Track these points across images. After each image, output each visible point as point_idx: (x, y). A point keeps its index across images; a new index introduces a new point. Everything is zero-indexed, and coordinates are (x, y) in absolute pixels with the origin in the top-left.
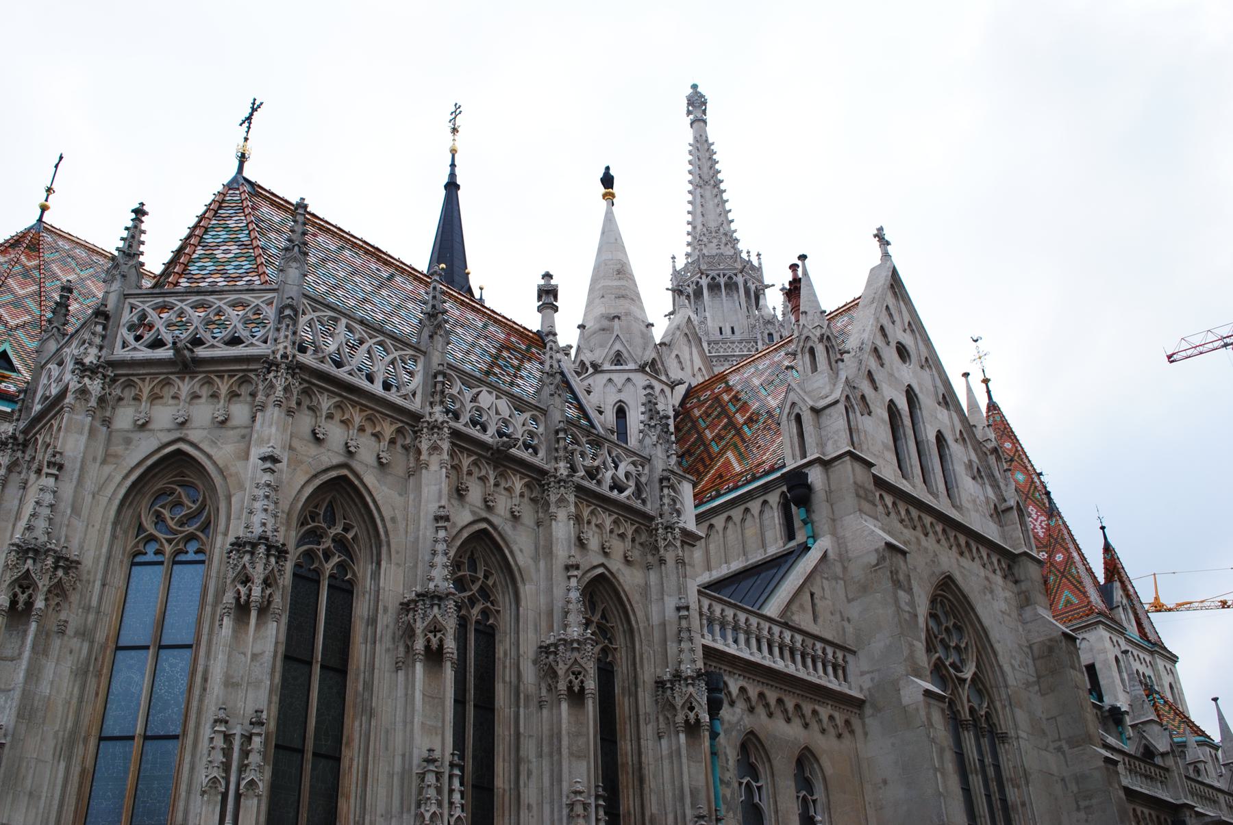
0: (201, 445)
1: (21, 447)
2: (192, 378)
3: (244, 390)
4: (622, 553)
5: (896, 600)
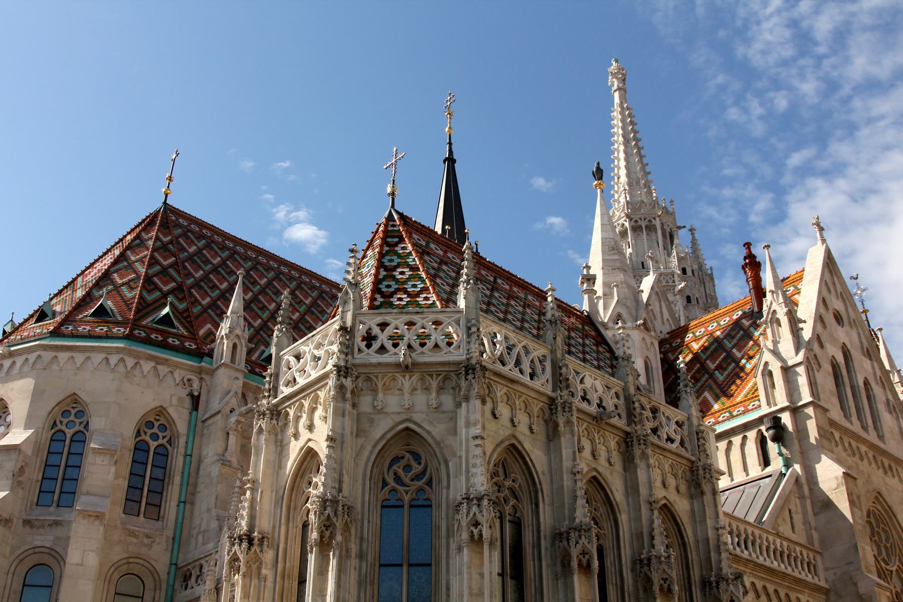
0: (423, 425)
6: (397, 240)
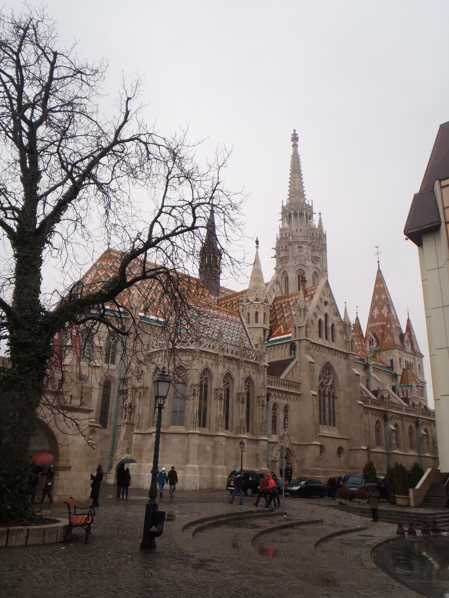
3: (191, 354)
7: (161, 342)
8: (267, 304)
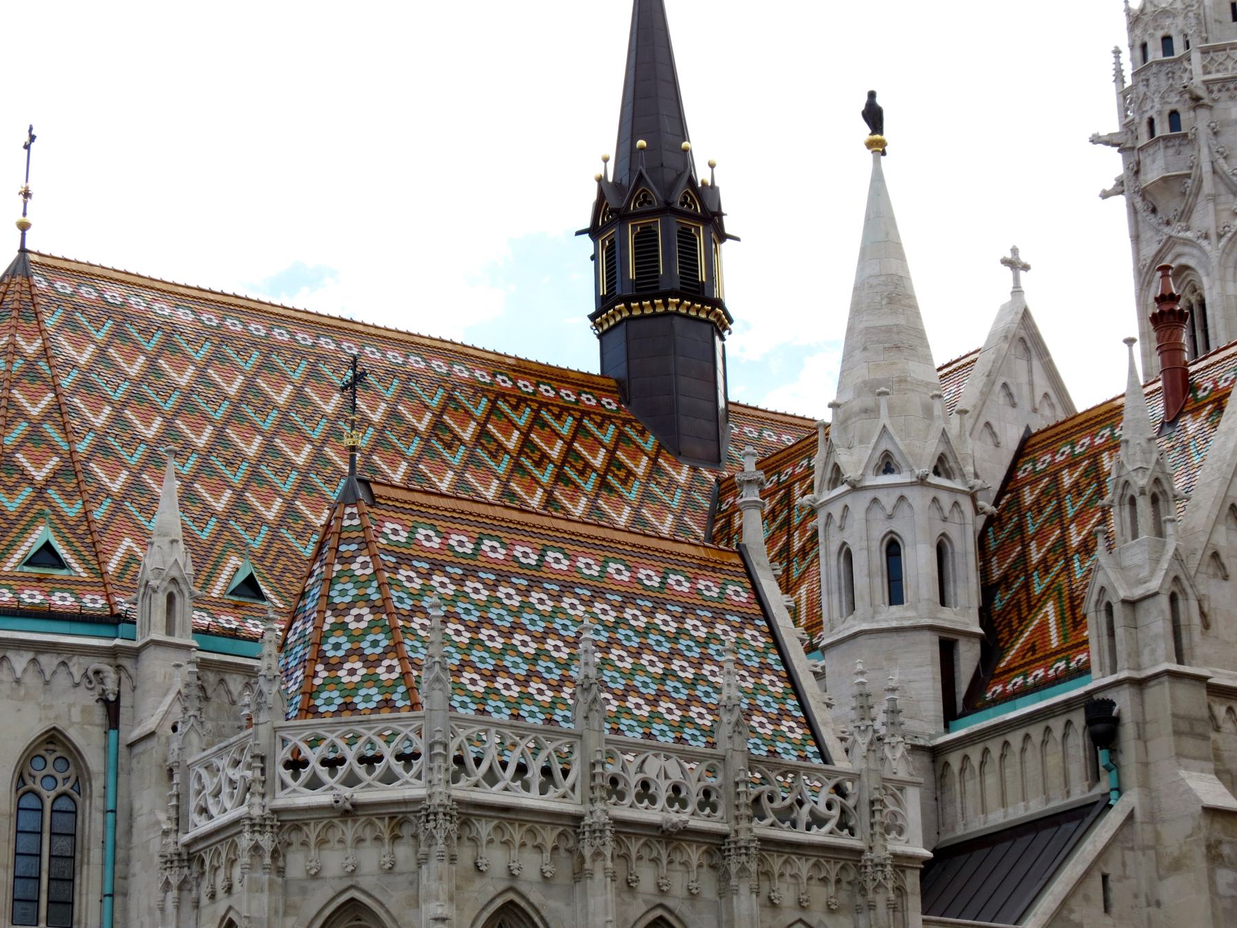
0: (373, 893)
1: (186, 864)
2: (355, 821)
4: (823, 900)
5: (1212, 883)
6: (354, 547)
7: (236, 774)
8: (957, 484)
